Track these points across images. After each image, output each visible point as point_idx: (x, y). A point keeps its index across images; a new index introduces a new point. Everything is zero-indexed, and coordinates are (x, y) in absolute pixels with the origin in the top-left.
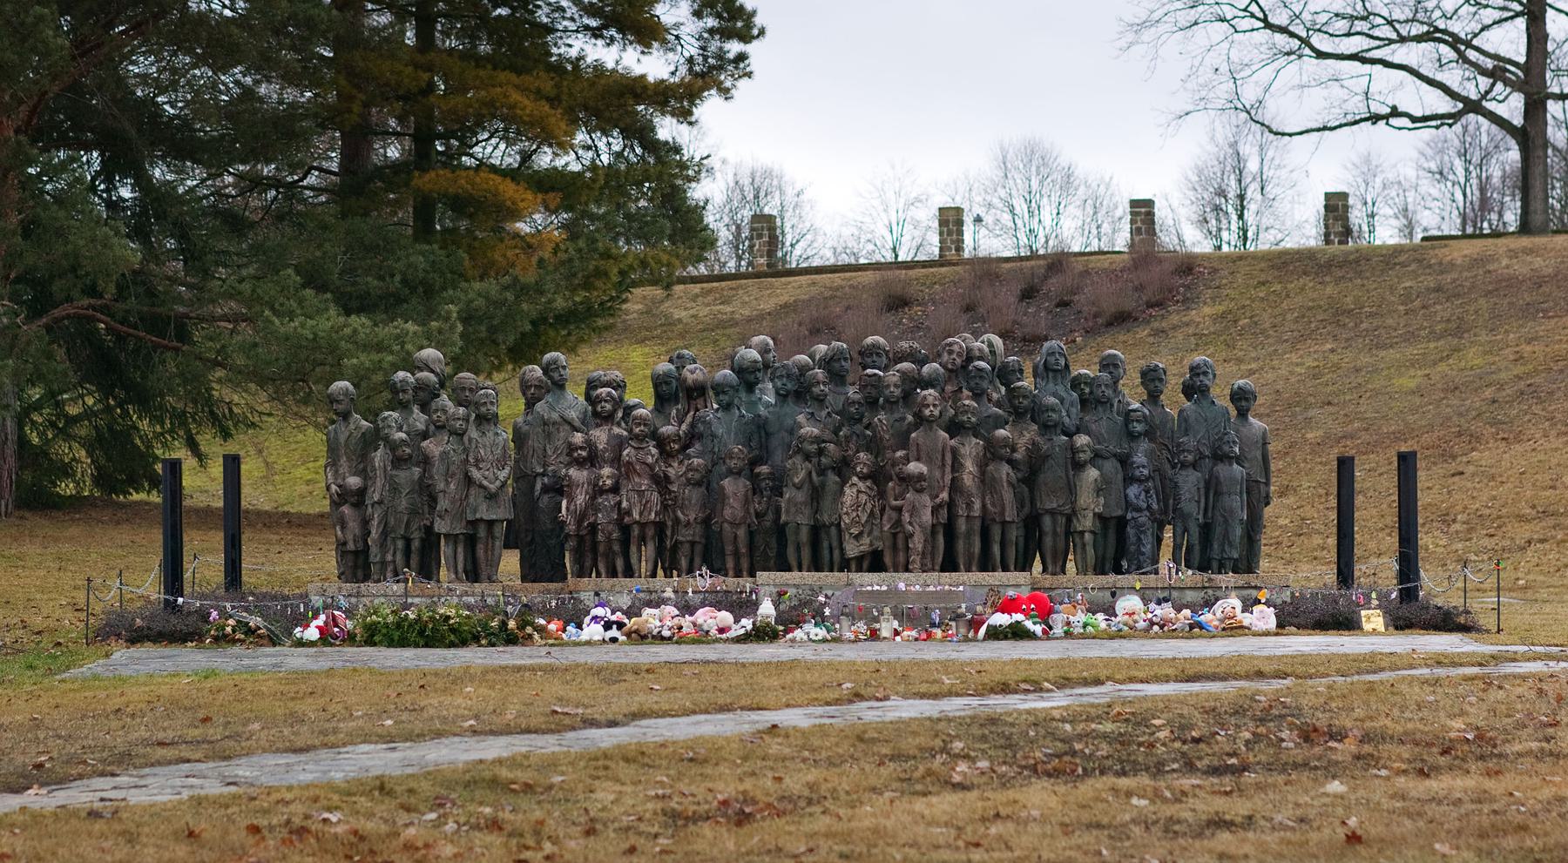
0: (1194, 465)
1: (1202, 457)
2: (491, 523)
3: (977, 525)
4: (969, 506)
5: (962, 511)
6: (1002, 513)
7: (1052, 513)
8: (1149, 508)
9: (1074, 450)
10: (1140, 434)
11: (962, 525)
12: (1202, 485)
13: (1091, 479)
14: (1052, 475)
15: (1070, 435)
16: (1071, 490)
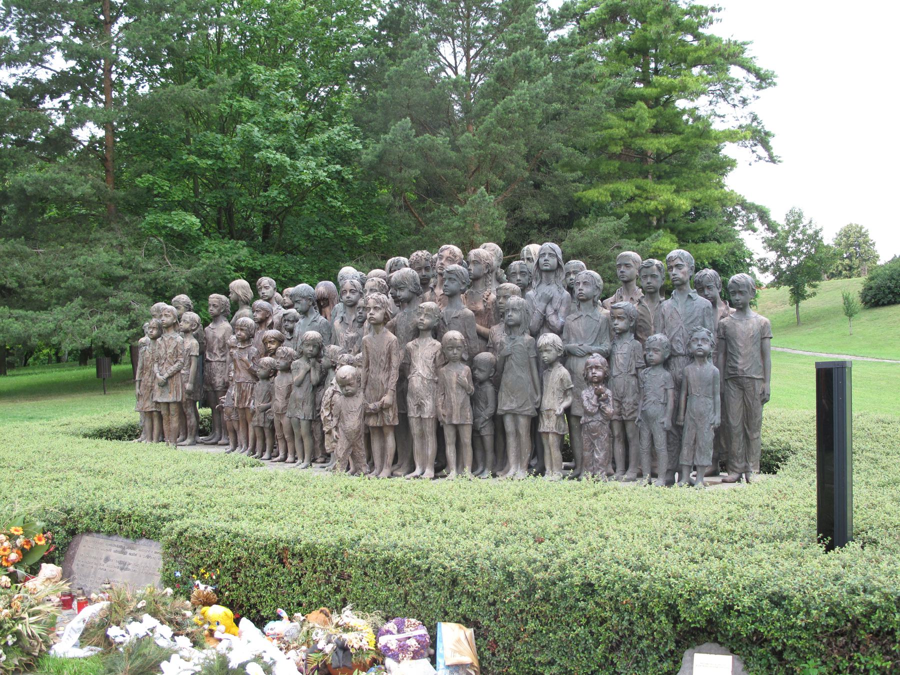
0: (666, 364)
1: (673, 355)
2: (168, 404)
3: (430, 429)
4: (420, 407)
5: (413, 413)
6: (451, 416)
7: (515, 415)
8: (601, 410)
9: (539, 350)
10: (622, 333)
11: (415, 429)
12: (671, 385)
13: (557, 379)
14: (517, 375)
15: (535, 335)
16: (540, 388)
